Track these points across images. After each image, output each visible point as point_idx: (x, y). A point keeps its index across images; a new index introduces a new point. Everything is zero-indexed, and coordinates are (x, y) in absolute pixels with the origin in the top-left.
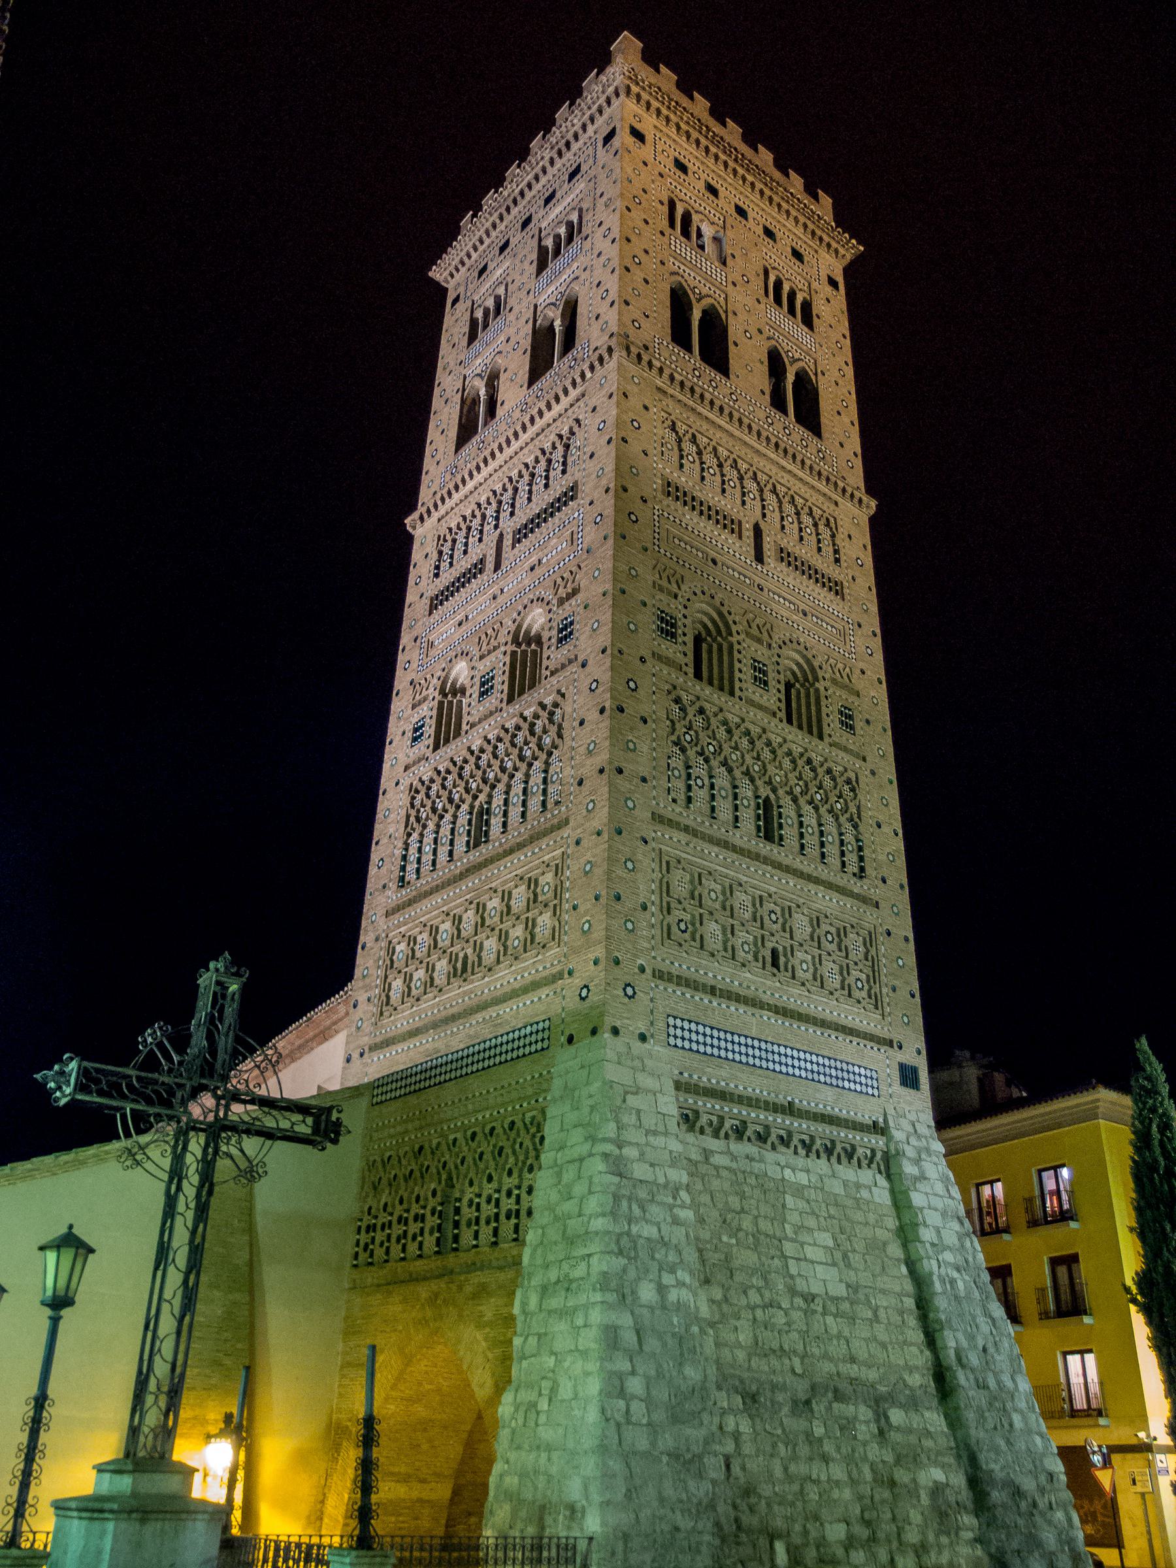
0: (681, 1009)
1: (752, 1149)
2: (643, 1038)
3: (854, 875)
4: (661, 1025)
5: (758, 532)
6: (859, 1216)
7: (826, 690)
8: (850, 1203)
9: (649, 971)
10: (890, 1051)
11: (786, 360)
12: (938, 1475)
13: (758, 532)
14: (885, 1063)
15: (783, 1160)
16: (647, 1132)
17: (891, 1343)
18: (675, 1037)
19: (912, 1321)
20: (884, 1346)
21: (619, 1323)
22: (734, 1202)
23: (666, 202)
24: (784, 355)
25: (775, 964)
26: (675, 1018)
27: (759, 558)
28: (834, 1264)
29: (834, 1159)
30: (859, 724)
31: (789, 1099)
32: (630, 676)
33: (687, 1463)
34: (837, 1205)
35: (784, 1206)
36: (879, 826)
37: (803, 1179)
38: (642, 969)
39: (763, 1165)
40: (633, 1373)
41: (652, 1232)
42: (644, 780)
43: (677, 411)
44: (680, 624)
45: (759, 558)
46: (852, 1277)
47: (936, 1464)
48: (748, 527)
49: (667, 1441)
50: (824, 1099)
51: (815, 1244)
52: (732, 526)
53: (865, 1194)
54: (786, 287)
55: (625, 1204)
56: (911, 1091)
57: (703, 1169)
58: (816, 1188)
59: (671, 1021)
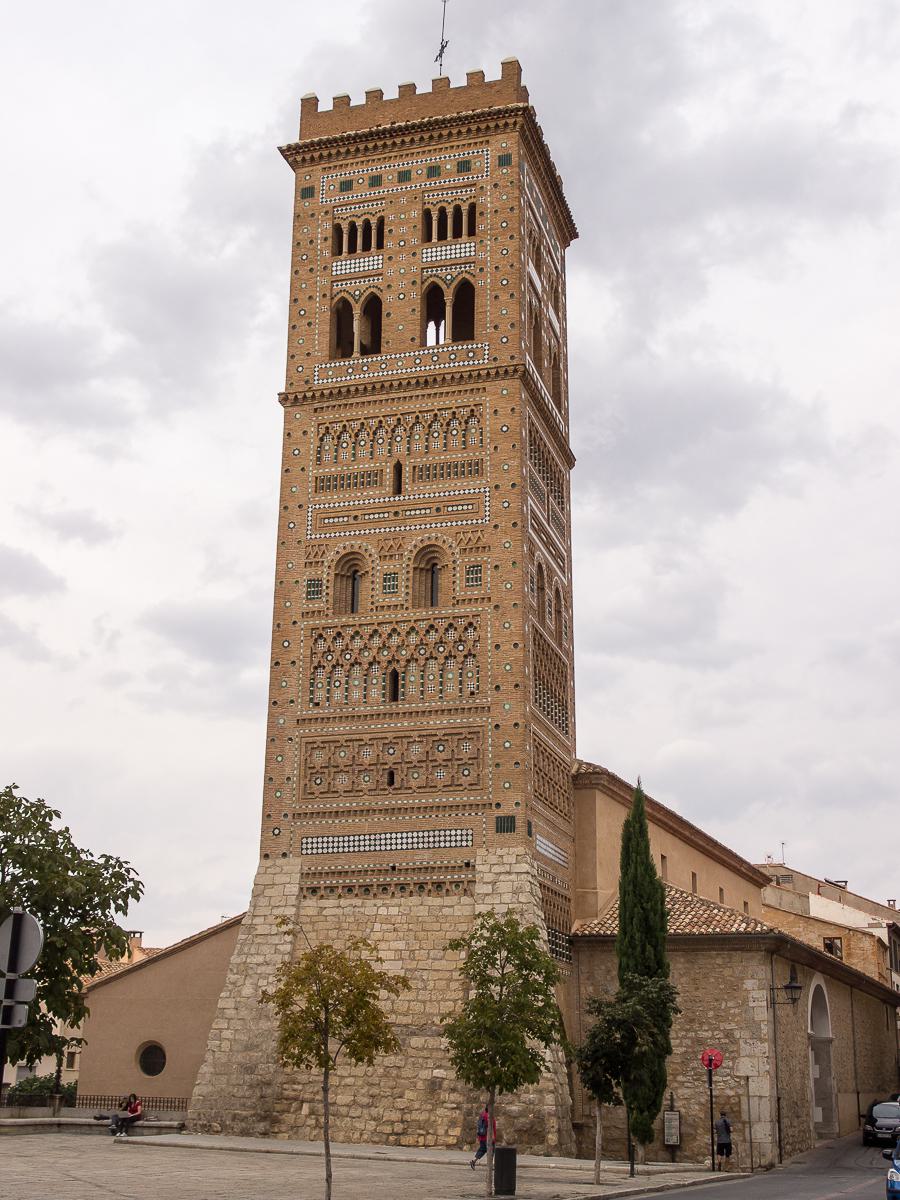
0: (312, 831)
1: (358, 902)
2: (284, 855)
3: (472, 693)
4: (298, 845)
5: (398, 468)
6: (436, 926)
7: (454, 562)
8: (427, 919)
9: (290, 817)
10: (488, 811)
11: (444, 287)
12: (438, 1073)
13: (398, 468)
14: (486, 821)
15: (379, 902)
16: (274, 907)
17: (430, 1001)
18: (307, 849)
19: (454, 985)
20: (424, 1002)
21: (226, 1006)
22: (333, 934)
23: (329, 232)
24: (440, 283)
25: (391, 782)
26: (307, 838)
27: (398, 490)
28: (401, 959)
29: (423, 894)
30: (488, 575)
31: (391, 865)
32: (284, 639)
33: (249, 1069)
34: (418, 922)
35: (372, 931)
36: (497, 647)
37: (394, 911)
38: (286, 815)
39: (362, 910)
40: (228, 1029)
41: (260, 959)
42: (292, 702)
43: (328, 416)
44: (325, 582)
45: (398, 490)
46: (413, 965)
47: (439, 1067)
48: (389, 471)
49: (239, 1058)
50: (424, 858)
51: (389, 950)
52: (371, 479)
53: (446, 911)
54: (450, 210)
55: (246, 949)
56: (507, 835)
57: (314, 919)
58: (403, 914)
59: (304, 841)
